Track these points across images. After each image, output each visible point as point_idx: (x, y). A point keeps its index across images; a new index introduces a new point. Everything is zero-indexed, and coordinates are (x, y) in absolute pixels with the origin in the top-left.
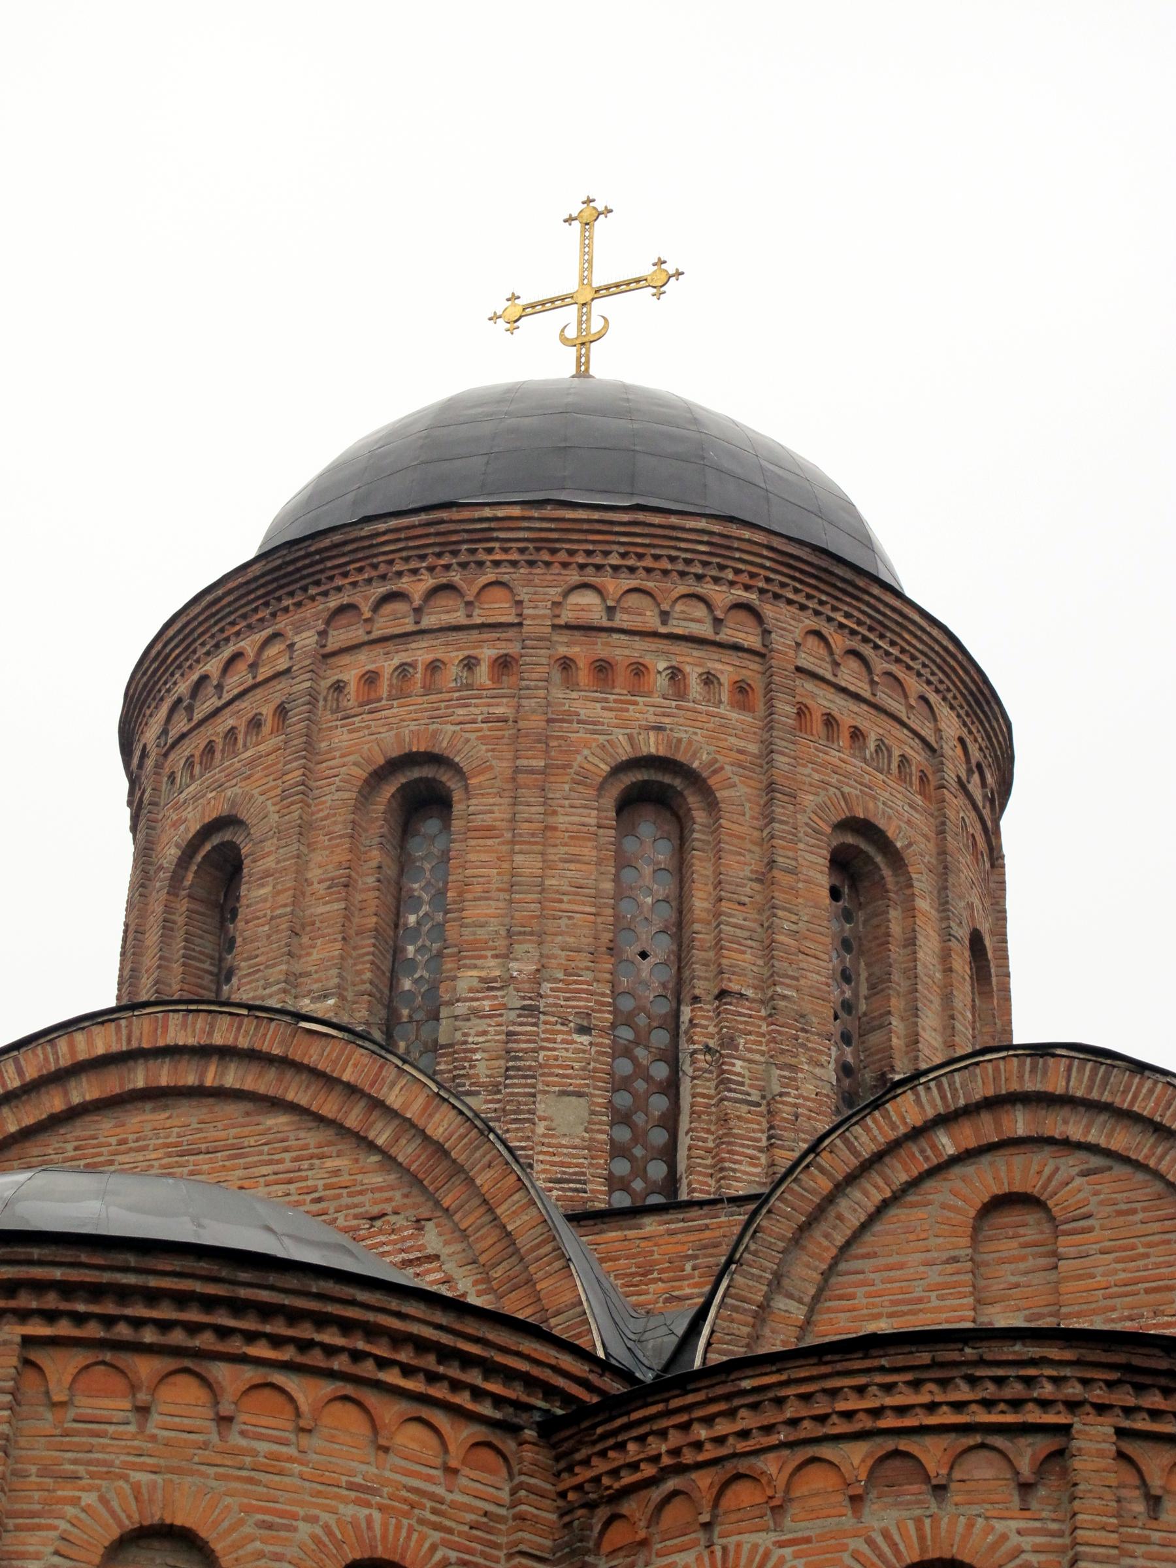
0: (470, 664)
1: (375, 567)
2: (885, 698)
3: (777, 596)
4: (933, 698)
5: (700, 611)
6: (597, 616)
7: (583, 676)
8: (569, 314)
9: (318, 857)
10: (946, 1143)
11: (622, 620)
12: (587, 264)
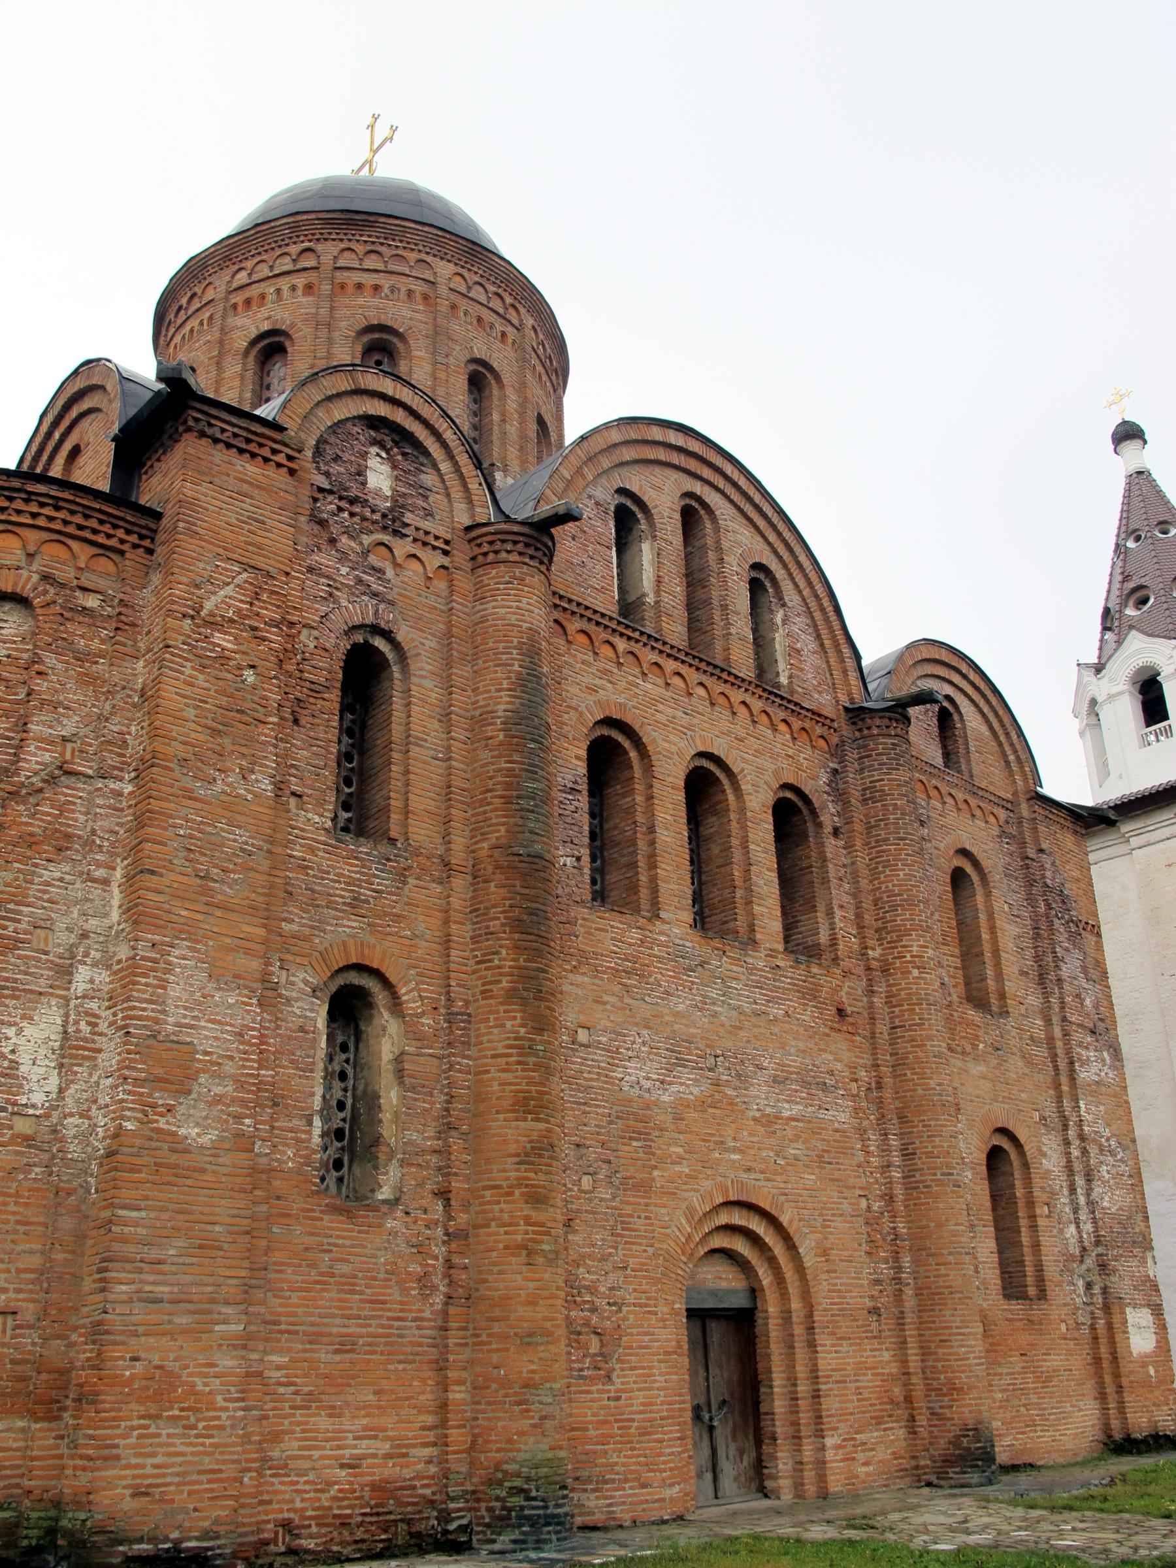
0: (201, 323)
2: (392, 267)
3: (326, 240)
4: (429, 259)
7: (240, 309)
10: (57, 435)
11: (255, 277)
12: (372, 142)
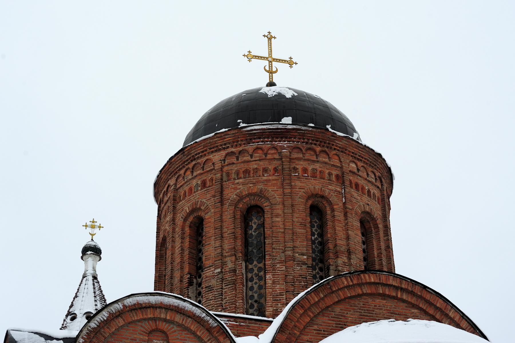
1: (304, 139)
5: (373, 176)
6: (355, 170)
8: (266, 63)
9: (296, 215)
